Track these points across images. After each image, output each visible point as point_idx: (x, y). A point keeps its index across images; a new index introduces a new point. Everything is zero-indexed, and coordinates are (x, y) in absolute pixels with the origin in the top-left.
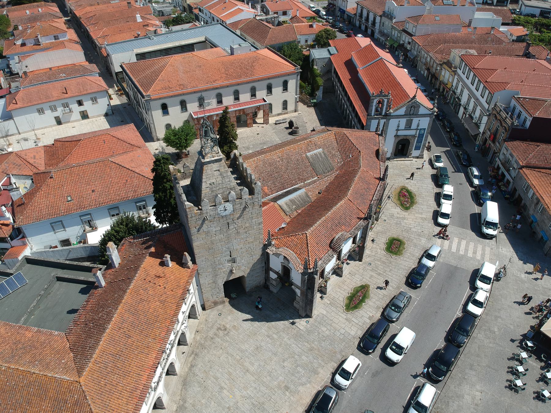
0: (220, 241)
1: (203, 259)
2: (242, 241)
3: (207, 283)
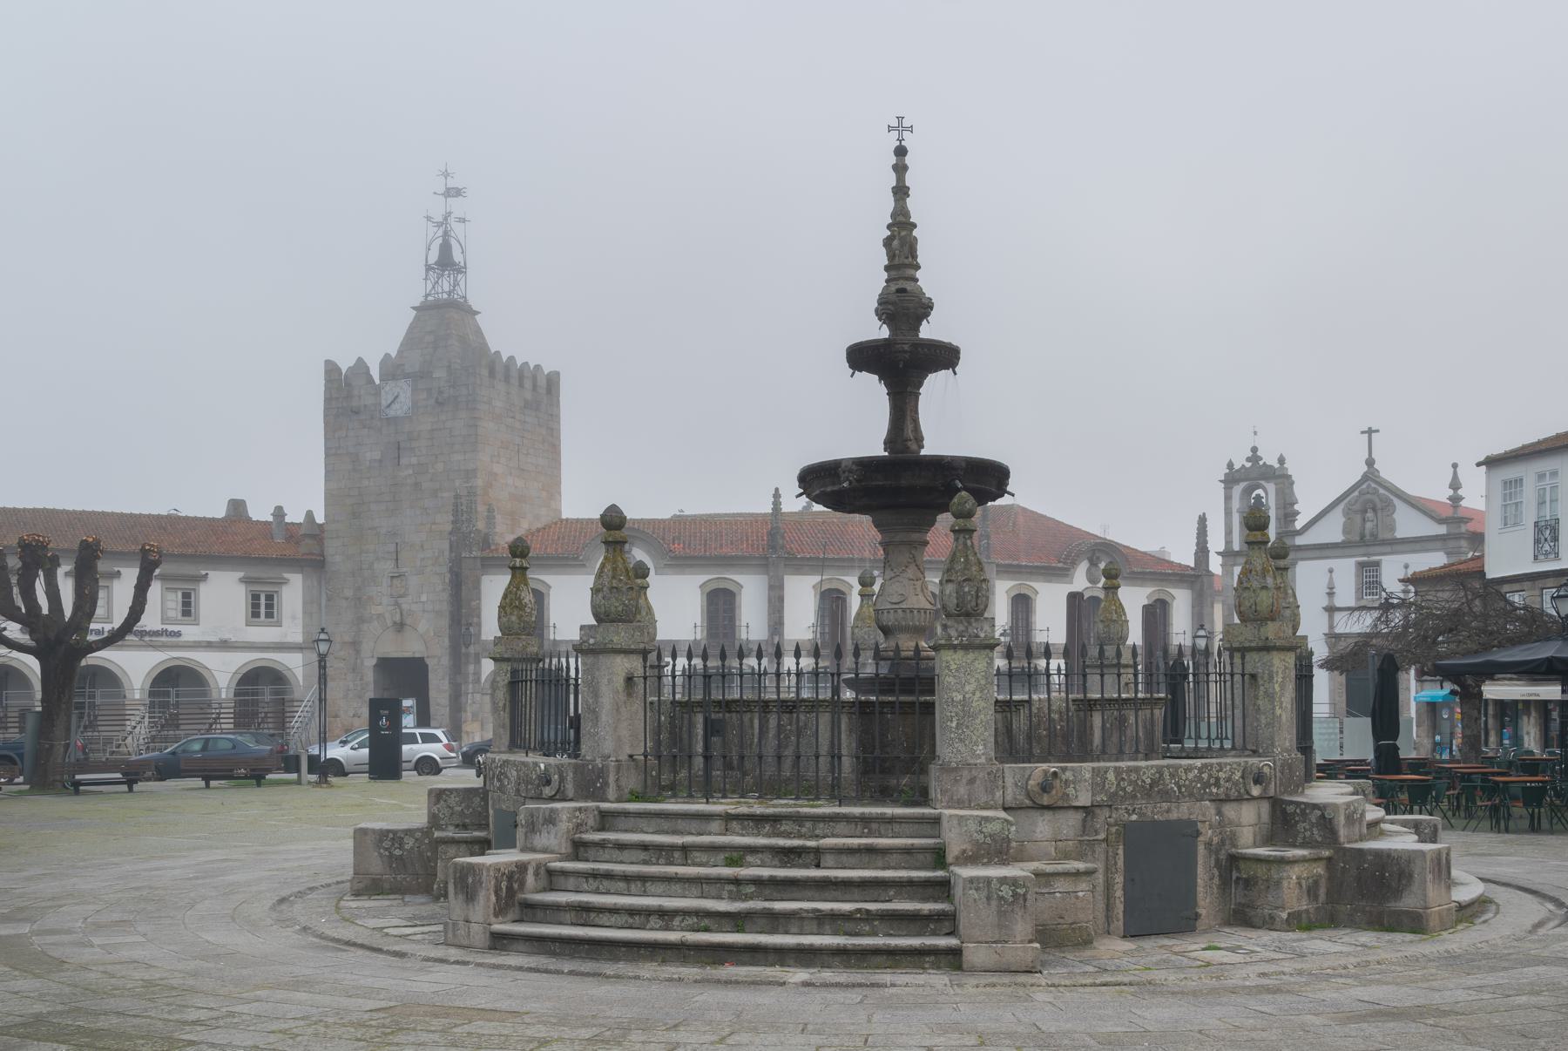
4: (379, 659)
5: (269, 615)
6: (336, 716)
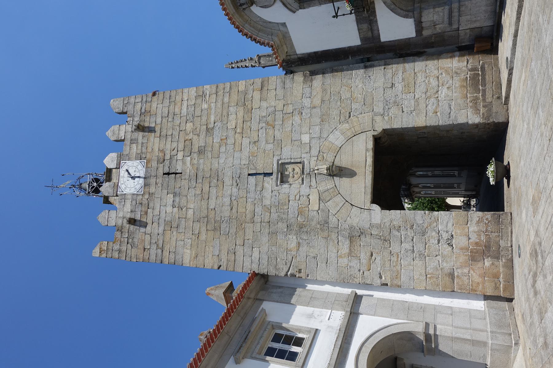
0: (204, 197)
1: (240, 250)
2: (230, 141)
3: (344, 261)
4: (374, 201)
5: (299, 342)
6: (451, 275)
